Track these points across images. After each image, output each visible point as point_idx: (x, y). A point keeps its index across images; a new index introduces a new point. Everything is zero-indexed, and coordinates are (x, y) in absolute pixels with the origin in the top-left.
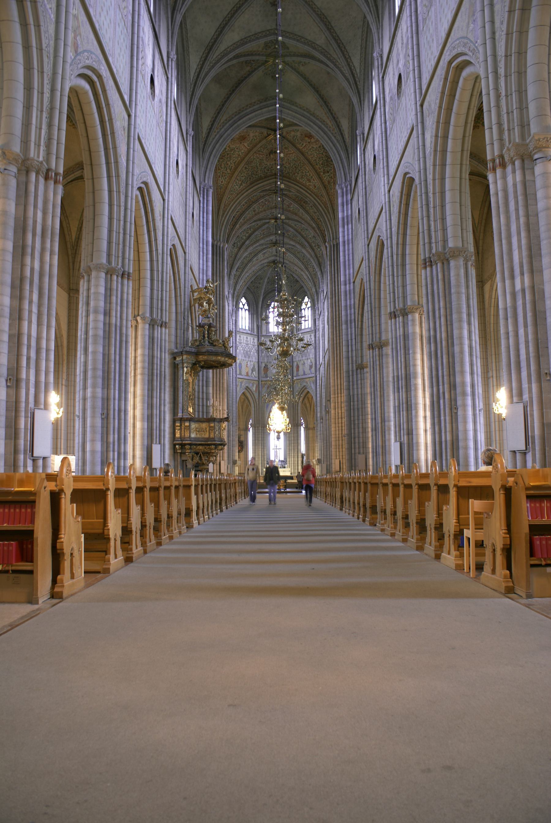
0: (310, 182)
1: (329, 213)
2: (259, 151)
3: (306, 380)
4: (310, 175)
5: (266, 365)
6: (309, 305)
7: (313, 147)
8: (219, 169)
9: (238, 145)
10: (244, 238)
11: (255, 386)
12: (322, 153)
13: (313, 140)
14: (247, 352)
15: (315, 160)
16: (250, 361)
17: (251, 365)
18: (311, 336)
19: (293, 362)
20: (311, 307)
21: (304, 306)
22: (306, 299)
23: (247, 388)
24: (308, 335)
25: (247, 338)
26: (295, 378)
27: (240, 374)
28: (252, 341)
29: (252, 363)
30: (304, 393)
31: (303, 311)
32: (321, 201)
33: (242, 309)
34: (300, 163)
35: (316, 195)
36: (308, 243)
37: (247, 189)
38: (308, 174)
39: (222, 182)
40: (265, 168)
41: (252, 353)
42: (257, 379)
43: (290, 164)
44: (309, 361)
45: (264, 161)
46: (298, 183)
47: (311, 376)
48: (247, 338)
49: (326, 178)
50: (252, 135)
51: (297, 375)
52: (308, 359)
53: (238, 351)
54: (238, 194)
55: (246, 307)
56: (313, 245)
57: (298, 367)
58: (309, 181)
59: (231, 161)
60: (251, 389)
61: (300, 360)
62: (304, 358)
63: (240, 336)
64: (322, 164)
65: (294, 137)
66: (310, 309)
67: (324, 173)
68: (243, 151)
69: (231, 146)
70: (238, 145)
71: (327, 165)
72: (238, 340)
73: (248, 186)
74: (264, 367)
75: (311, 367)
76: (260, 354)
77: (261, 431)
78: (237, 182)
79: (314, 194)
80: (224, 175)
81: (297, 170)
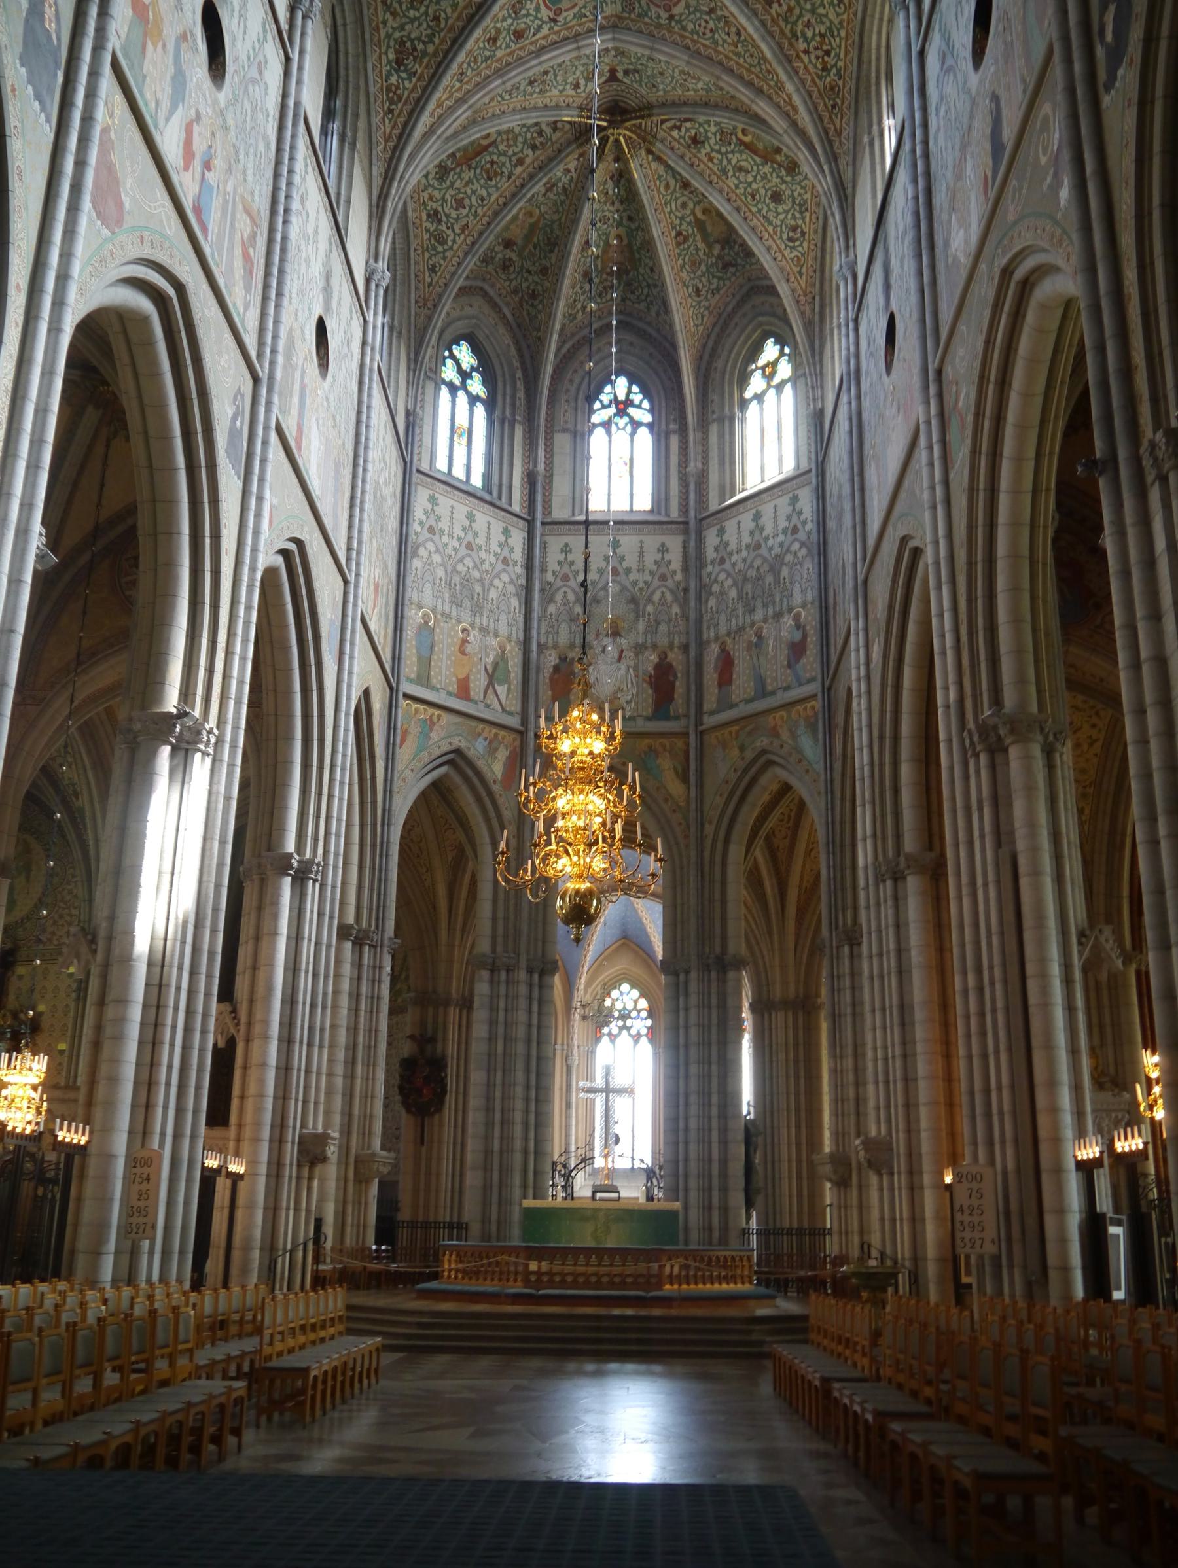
3: (770, 720)
5: (563, 659)
6: (785, 370)
11: (502, 754)
14: (467, 581)
16: (484, 631)
17: (485, 648)
18: (795, 500)
19: (702, 645)
20: (794, 379)
21: (756, 383)
22: (770, 350)
23: (457, 759)
24: (783, 503)
25: (471, 517)
26: (709, 721)
27: (424, 679)
28: (497, 536)
29: (494, 642)
30: (760, 797)
31: (753, 406)
33: (453, 389)
41: (493, 594)
42: (514, 722)
44: (788, 621)
47: (796, 693)
48: (471, 517)
51: (725, 704)
52: (778, 615)
53: (416, 563)
55: (476, 386)
57: (726, 664)
60: (481, 764)
61: (740, 630)
62: (759, 615)
63: (433, 500)
66: (788, 388)
72: (418, 513)
74: (556, 668)
75: (797, 650)
76: (536, 604)
77: (523, 990)
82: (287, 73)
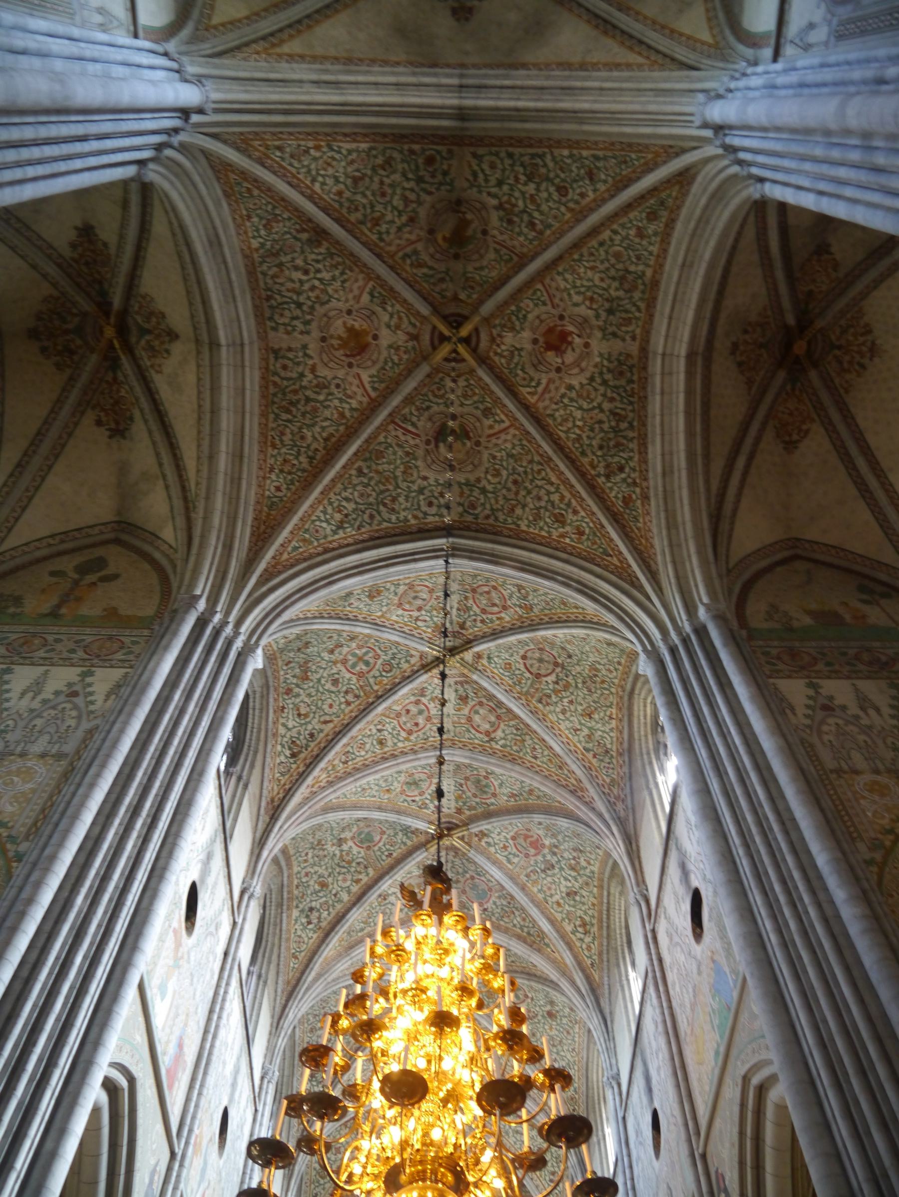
0: (563, 523)
1: (640, 588)
2: (405, 419)
4: (562, 498)
7: (570, 388)
8: (274, 446)
9: (341, 373)
10: (345, 897)
12: (600, 407)
13: (570, 357)
15: (579, 438)
32: (606, 568)
34: (531, 462)
35: (585, 559)
36: (552, 922)
37: (360, 546)
38: (555, 498)
39: (278, 489)
40: (421, 491)
43: (497, 474)
45: (420, 463)
46: (526, 540)
49: (615, 491)
50: (386, 338)
54: (326, 551)
56: (569, 928)
58: (560, 520)
59: (317, 429)
64: (601, 447)
65: (512, 352)
67: (608, 477)
68: (354, 404)
69: (323, 372)
70: (341, 373)
71: (617, 445)
73: (363, 541)
78: (330, 510)
79: (579, 556)
80: (287, 468)
81: (523, 493)
82: (254, 1120)
